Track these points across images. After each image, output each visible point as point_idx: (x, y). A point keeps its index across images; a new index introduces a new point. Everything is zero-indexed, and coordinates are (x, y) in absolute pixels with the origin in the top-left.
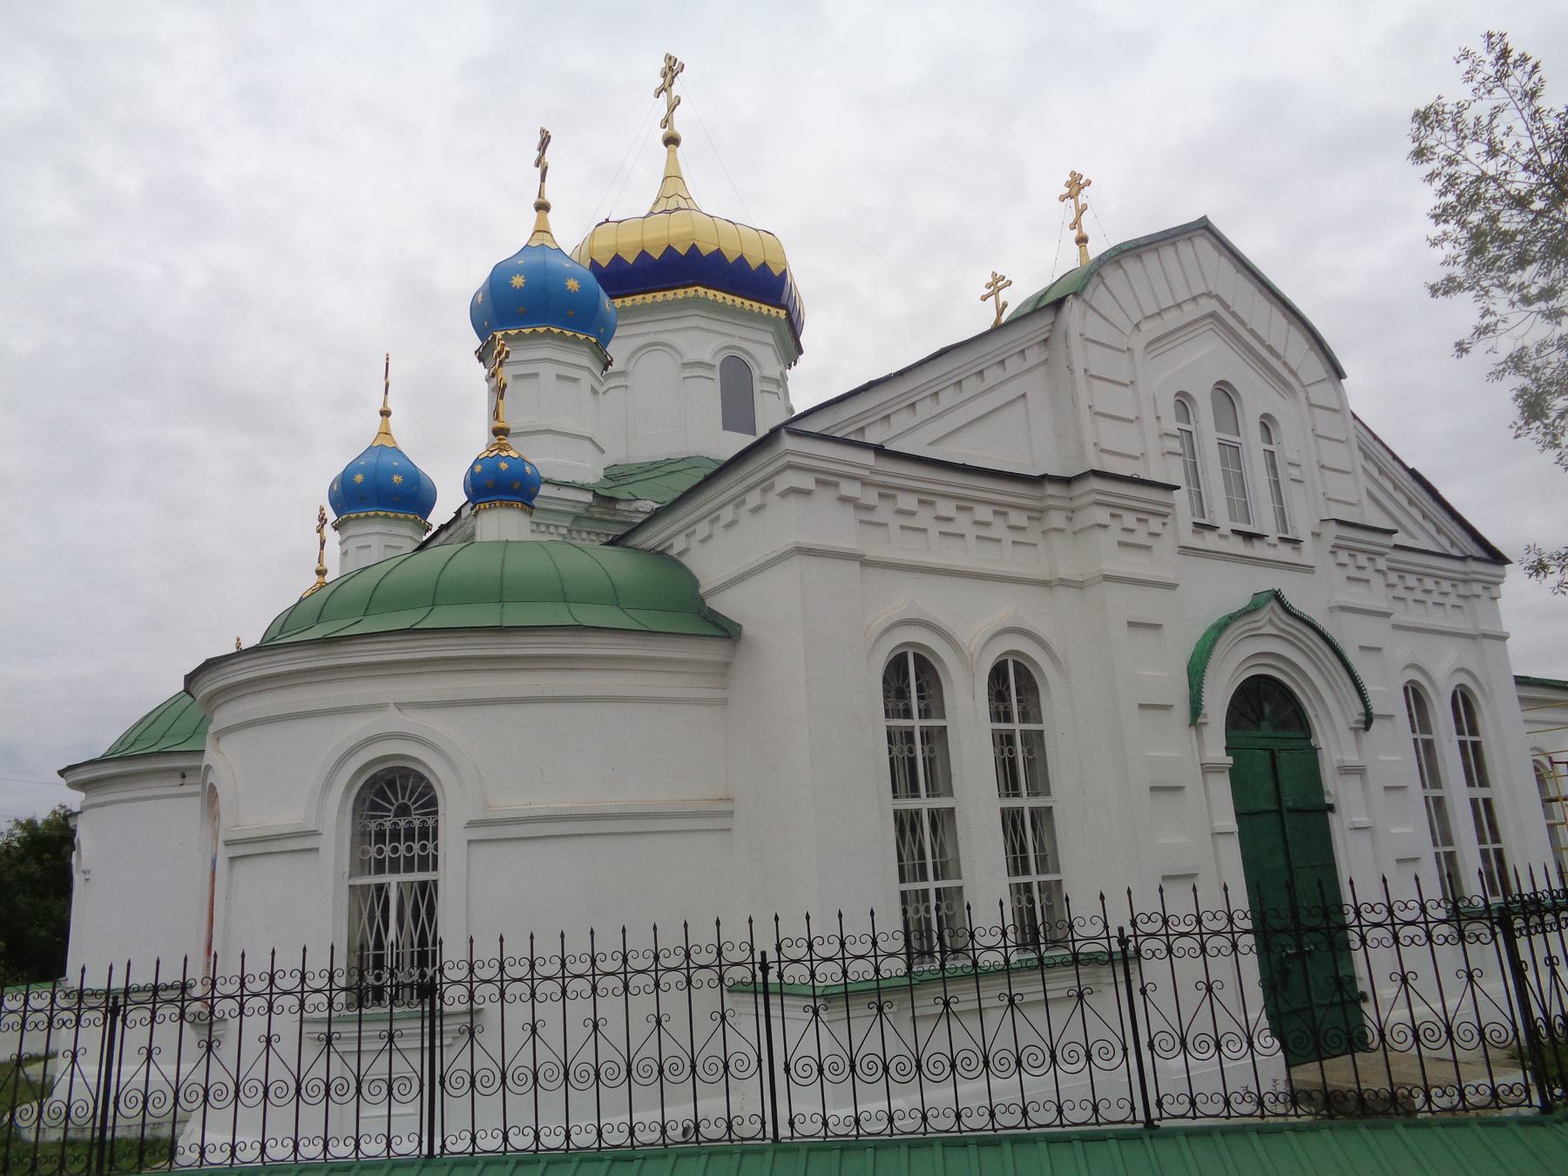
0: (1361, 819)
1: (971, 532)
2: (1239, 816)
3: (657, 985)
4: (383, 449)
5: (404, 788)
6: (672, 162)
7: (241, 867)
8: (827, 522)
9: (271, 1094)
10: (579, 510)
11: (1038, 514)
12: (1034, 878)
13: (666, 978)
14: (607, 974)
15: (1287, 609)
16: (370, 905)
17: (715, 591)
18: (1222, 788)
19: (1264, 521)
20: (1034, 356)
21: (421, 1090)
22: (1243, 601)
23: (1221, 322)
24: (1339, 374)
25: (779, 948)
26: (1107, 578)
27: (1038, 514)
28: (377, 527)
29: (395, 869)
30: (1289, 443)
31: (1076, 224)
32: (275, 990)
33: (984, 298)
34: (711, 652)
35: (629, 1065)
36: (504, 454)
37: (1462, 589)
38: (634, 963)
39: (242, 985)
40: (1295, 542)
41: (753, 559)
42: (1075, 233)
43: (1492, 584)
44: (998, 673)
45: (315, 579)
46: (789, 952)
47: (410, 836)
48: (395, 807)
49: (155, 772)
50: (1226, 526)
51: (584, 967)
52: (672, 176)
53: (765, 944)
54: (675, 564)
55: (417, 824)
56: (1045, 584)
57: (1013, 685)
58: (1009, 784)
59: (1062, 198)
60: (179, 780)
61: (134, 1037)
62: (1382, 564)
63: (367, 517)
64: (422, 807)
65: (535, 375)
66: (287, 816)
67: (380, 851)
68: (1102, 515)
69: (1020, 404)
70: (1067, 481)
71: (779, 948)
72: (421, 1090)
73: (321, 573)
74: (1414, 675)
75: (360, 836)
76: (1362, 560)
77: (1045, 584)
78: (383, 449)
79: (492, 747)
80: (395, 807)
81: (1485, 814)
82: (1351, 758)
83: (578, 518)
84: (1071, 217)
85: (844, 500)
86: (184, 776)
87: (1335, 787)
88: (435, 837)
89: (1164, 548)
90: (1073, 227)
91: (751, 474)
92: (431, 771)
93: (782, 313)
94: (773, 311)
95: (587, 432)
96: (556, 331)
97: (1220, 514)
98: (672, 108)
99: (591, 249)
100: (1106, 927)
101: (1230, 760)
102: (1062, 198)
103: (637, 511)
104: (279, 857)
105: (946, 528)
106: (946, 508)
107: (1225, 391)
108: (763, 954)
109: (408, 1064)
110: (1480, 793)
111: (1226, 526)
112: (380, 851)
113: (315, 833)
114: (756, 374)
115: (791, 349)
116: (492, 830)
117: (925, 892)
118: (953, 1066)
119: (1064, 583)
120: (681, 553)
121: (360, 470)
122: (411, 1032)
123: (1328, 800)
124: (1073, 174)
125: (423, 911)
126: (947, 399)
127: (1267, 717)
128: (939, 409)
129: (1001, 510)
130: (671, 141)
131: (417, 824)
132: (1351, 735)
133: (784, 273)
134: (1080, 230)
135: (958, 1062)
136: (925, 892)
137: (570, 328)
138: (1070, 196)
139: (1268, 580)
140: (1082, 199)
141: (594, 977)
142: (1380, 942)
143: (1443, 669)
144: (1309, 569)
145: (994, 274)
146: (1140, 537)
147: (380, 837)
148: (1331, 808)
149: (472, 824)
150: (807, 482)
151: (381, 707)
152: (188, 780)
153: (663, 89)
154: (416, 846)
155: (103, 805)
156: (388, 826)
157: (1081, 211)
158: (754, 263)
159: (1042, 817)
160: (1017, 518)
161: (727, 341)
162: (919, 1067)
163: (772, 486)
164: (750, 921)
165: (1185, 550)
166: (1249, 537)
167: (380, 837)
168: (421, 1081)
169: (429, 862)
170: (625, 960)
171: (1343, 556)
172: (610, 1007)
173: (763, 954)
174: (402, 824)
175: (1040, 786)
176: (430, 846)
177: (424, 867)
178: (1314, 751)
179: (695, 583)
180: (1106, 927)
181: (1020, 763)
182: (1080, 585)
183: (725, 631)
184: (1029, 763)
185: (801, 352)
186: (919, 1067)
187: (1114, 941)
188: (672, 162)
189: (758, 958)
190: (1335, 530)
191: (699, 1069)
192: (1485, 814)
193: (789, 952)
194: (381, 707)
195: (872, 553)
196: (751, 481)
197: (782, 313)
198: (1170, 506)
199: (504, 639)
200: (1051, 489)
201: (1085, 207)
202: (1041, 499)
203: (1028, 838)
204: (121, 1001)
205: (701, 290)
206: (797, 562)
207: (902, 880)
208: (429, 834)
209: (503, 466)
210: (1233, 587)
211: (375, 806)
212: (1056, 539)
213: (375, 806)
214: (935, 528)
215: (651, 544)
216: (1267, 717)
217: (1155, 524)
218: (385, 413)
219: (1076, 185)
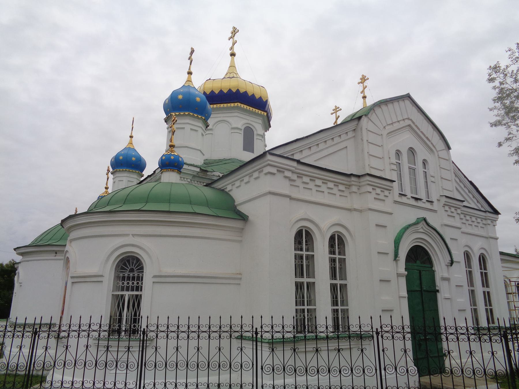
0: (447, 296)
1: (326, 191)
2: (409, 291)
3: (220, 337)
4: (130, 149)
5: (133, 263)
6: (232, 61)
7: (76, 286)
8: (280, 184)
9: (87, 365)
10: (195, 174)
12: (339, 307)
13: (223, 335)
14: (203, 332)
15: (428, 224)
16: (118, 302)
17: (241, 204)
18: (403, 282)
19: (422, 195)
20: (351, 134)
21: (138, 367)
22: (413, 221)
23: (412, 128)
24: (449, 148)
25: (262, 327)
26: (370, 209)
28: (126, 174)
29: (128, 290)
30: (432, 169)
31: (363, 92)
32: (90, 330)
33: (332, 114)
34: (238, 224)
35: (209, 363)
36: (173, 154)
37: (484, 222)
38: (213, 329)
39: (80, 327)
40: (432, 202)
41: (255, 194)
42: (362, 95)
43: (494, 221)
44: (332, 238)
45: (105, 190)
46: (265, 329)
47: (133, 278)
48: (130, 269)
49: (47, 251)
50: (409, 195)
51: (196, 329)
52: (232, 66)
53: (257, 325)
54: (227, 194)
55: (136, 275)
56: (349, 210)
57: (337, 243)
58: (333, 276)
59: (359, 83)
60: (55, 254)
61: (42, 343)
62: (459, 211)
63: (123, 171)
64: (138, 270)
65: (184, 128)
66: (93, 270)
67: (123, 283)
68: (370, 189)
69: (345, 150)
70: (359, 176)
71: (262, 327)
72: (138, 367)
73: (107, 188)
74: (483, 251)
75: (117, 277)
76: (453, 209)
77: (349, 210)
78: (130, 149)
79: (163, 251)
80: (130, 269)
81: (487, 296)
82: (446, 275)
83: (194, 176)
84: (361, 89)
85: (286, 177)
86: (56, 253)
87: (440, 284)
88: (142, 280)
89: (389, 201)
90: (362, 93)
91: (255, 167)
92: (142, 258)
93: (265, 114)
94: (263, 112)
95: (199, 148)
96: (192, 114)
98: (234, 44)
99: (204, 88)
100: (372, 328)
101: (406, 273)
102: (359, 83)
103: (214, 175)
104: (89, 283)
105: (331, 191)
106: (319, 182)
107: (412, 151)
108: (256, 329)
109: (134, 357)
110: (486, 290)
111: (409, 195)
112: (123, 283)
113: (102, 276)
114: (255, 133)
115: (267, 126)
116: (162, 279)
117: (304, 310)
118: (318, 371)
119: (355, 210)
120: (229, 191)
121: (122, 155)
122: (135, 345)
123: (437, 288)
124: (363, 75)
125: (136, 305)
126: (322, 146)
127: (419, 259)
128: (318, 150)
129: (336, 184)
130: (233, 55)
131: (136, 275)
132: (446, 267)
133: (267, 101)
134: (364, 94)
135: (320, 370)
136: (304, 310)
137: (196, 113)
138: (361, 83)
140: (365, 84)
141: (199, 332)
142: (463, 340)
143: (477, 247)
145: (336, 106)
146: (381, 197)
147: (123, 278)
148: (438, 291)
149: (155, 277)
150: (274, 170)
151: (127, 235)
152: (57, 254)
153: (231, 38)
154: (135, 283)
155: (28, 261)
156: (126, 275)
157: (365, 88)
158: (257, 97)
159: (344, 287)
160: (341, 187)
161: (246, 121)
162: (306, 371)
163: (262, 171)
164: (253, 317)
165: (396, 202)
166: (417, 199)
167: (123, 278)
168: (138, 364)
169: (139, 288)
170: (210, 328)
171: (447, 208)
172: (204, 343)
173: (256, 329)
174: (131, 275)
175: (343, 277)
176: (140, 283)
177: (137, 290)
178: (434, 271)
179: (234, 201)
180: (372, 328)
181: (337, 269)
182: (360, 211)
183: (243, 218)
184: (340, 269)
185: (270, 127)
186: (306, 371)
187: (374, 333)
188: (232, 61)
189: (254, 330)
191: (232, 366)
192: (487, 296)
193: (265, 329)
194: (127, 235)
195: (294, 195)
196: (255, 169)
197: (265, 114)
198: (392, 187)
199: (169, 215)
200: (353, 179)
201: (366, 87)
202: (350, 182)
203: (338, 294)
204: (38, 330)
205: (239, 104)
206: (269, 197)
207: (296, 305)
208: (140, 279)
209: (172, 157)
210: (411, 215)
211: (122, 268)
212: (354, 195)
213: (122, 268)
214: (315, 189)
215: (220, 187)
216: (419, 259)
217: (386, 193)
219: (364, 79)
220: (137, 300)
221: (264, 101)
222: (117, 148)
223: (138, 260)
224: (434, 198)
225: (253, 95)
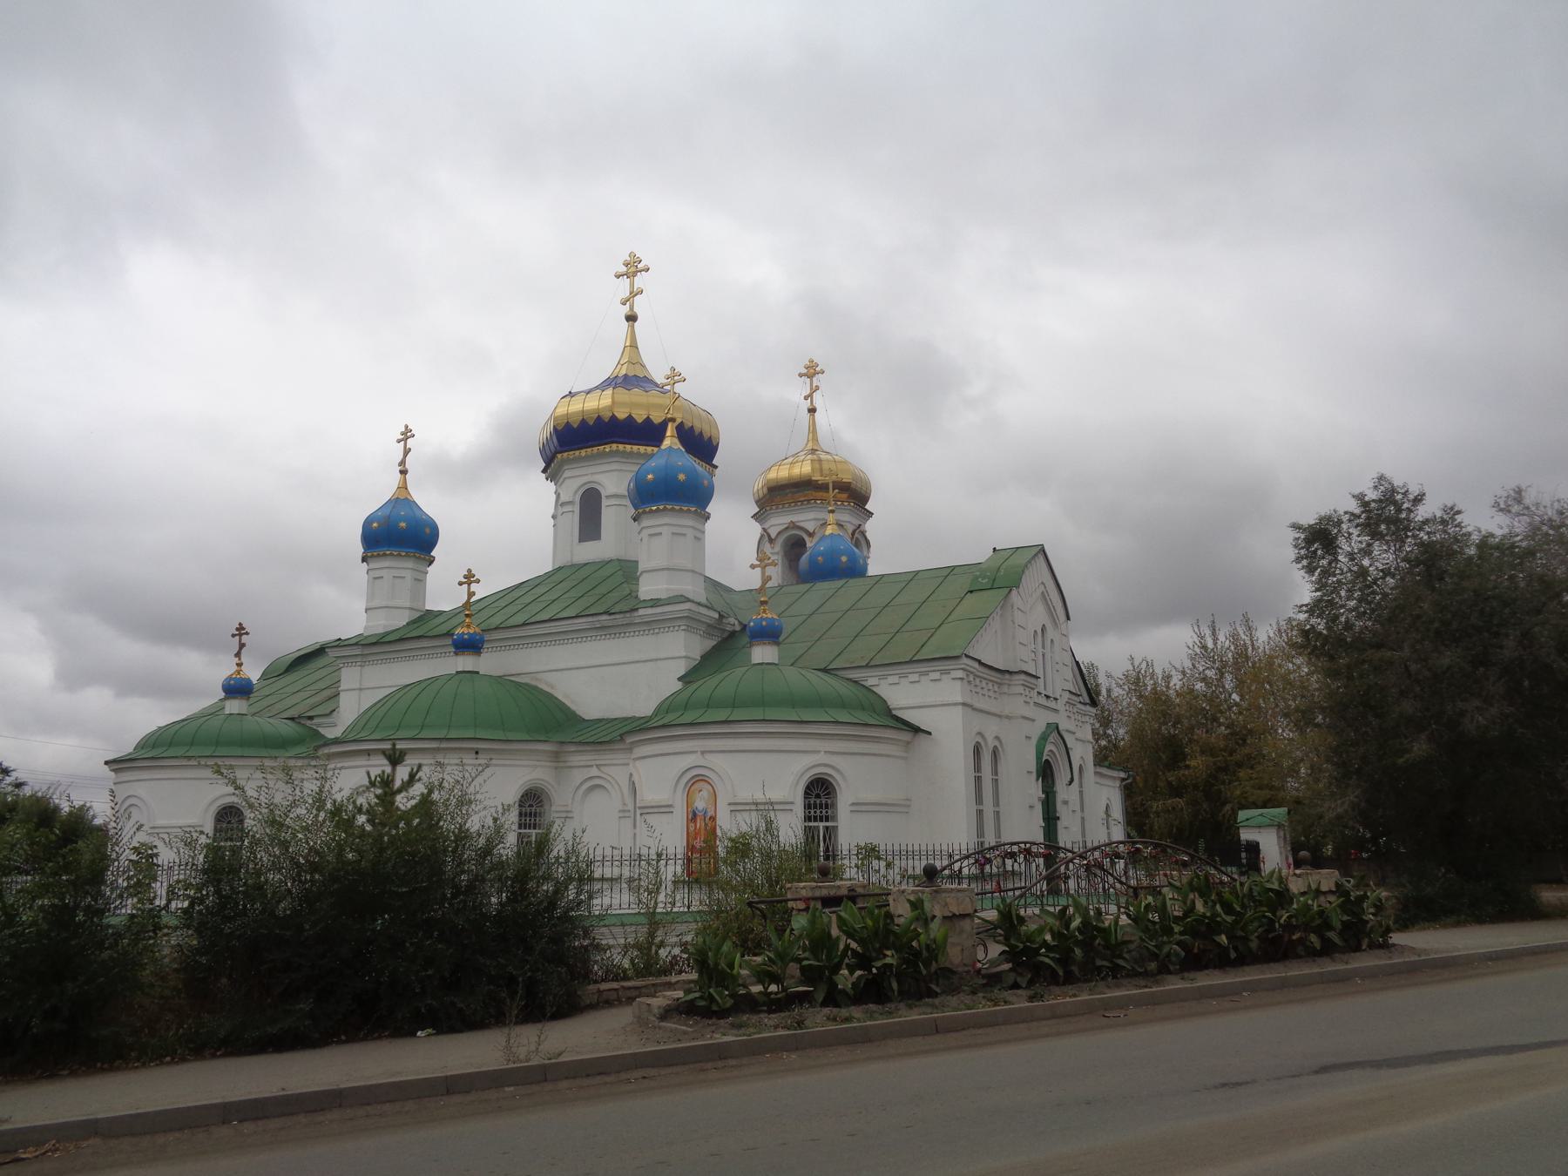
4: (402, 500)
11: (1000, 684)
27: (1000, 684)
28: (410, 564)
31: (809, 397)
34: (905, 736)
41: (930, 700)
48: (820, 792)
52: (634, 345)
59: (801, 375)
68: (1020, 689)
75: (808, 806)
78: (402, 500)
80: (820, 792)
95: (690, 566)
102: (801, 375)
107: (1043, 629)
116: (858, 807)
119: (1008, 717)
130: (632, 318)
139: (1052, 718)
144: (1056, 711)
153: (627, 274)
169: (834, 818)
190: (1067, 695)
195: (977, 705)
201: (817, 388)
208: (834, 805)
210: (1043, 719)
218: (404, 472)
220: (830, 833)
222: (376, 495)
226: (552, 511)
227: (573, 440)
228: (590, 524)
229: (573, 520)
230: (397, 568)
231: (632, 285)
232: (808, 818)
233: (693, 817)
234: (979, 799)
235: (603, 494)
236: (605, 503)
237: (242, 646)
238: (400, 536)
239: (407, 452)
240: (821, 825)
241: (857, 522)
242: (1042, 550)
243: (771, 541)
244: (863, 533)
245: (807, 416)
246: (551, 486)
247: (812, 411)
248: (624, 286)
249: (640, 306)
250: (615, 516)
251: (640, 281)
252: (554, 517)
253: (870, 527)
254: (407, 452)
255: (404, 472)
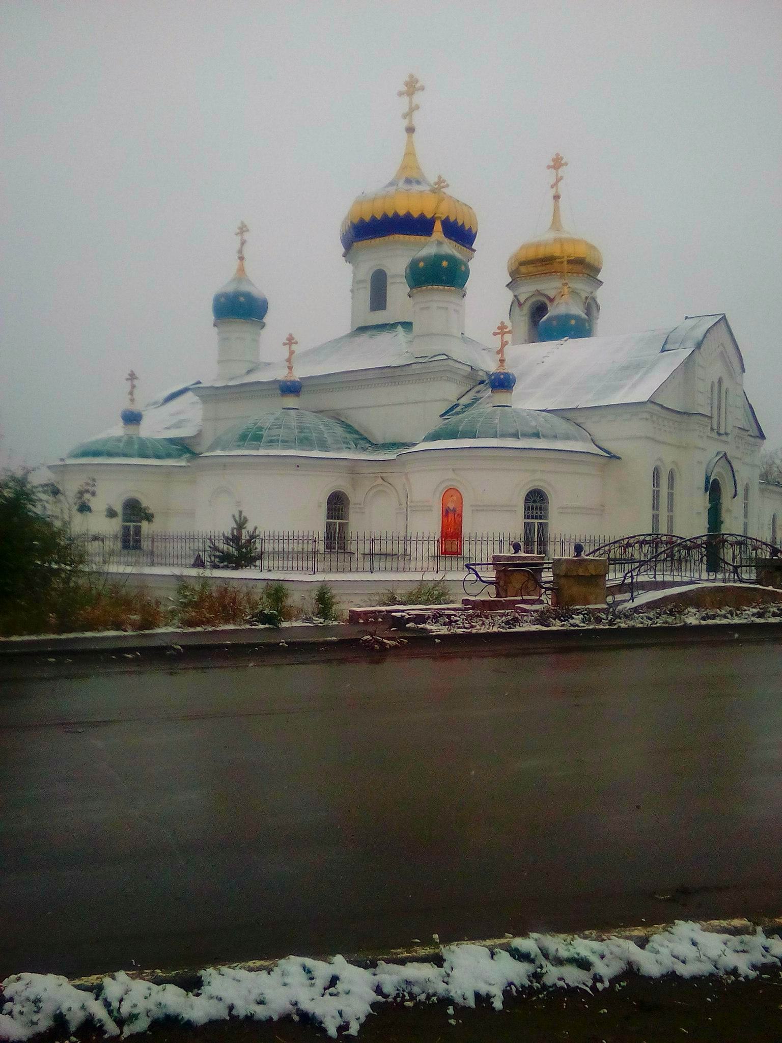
6: (410, 144)
23: (723, 355)
24: (743, 371)
48: (536, 501)
52: (410, 153)
59: (549, 167)
75: (527, 508)
80: (536, 501)
84: (553, 181)
97: (715, 427)
102: (549, 167)
107: (720, 381)
113: (515, 506)
130: (410, 130)
157: (559, 180)
169: (546, 518)
188: (410, 144)
190: (737, 431)
200: (686, 417)
208: (546, 509)
218: (241, 258)
221: (474, 232)
223: (530, 492)
224: (728, 431)
225: (463, 224)
226: (350, 287)
227: (368, 230)
228: (379, 300)
229: (365, 295)
230: (240, 330)
231: (411, 102)
232: (527, 517)
233: (446, 513)
234: (656, 506)
235: (388, 274)
236: (389, 281)
237: (133, 387)
238: (240, 309)
239: (243, 243)
240: (536, 521)
241: (589, 290)
242: (724, 318)
243: (520, 305)
244: (594, 299)
245: (552, 202)
246: (348, 268)
247: (557, 197)
248: (403, 104)
249: (418, 120)
250: (398, 291)
251: (418, 98)
252: (352, 291)
253: (601, 295)
254: (243, 243)
255: (241, 258)
